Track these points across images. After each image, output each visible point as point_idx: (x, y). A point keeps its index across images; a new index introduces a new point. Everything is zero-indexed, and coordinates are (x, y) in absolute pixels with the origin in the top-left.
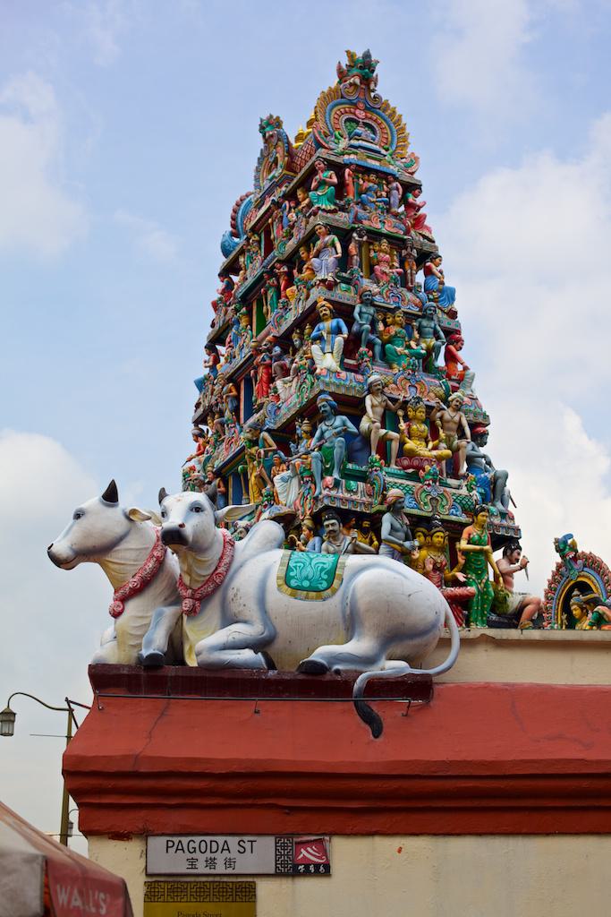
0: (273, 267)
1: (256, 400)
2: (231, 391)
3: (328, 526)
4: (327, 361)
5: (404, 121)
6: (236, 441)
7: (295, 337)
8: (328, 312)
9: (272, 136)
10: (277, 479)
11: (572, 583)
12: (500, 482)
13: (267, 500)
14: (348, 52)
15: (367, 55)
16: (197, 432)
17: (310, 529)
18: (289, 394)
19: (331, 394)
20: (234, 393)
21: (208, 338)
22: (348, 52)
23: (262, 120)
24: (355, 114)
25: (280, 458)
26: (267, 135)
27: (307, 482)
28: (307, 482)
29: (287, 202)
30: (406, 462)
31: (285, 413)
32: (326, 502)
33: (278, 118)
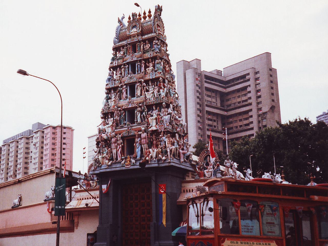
3: (169, 135)
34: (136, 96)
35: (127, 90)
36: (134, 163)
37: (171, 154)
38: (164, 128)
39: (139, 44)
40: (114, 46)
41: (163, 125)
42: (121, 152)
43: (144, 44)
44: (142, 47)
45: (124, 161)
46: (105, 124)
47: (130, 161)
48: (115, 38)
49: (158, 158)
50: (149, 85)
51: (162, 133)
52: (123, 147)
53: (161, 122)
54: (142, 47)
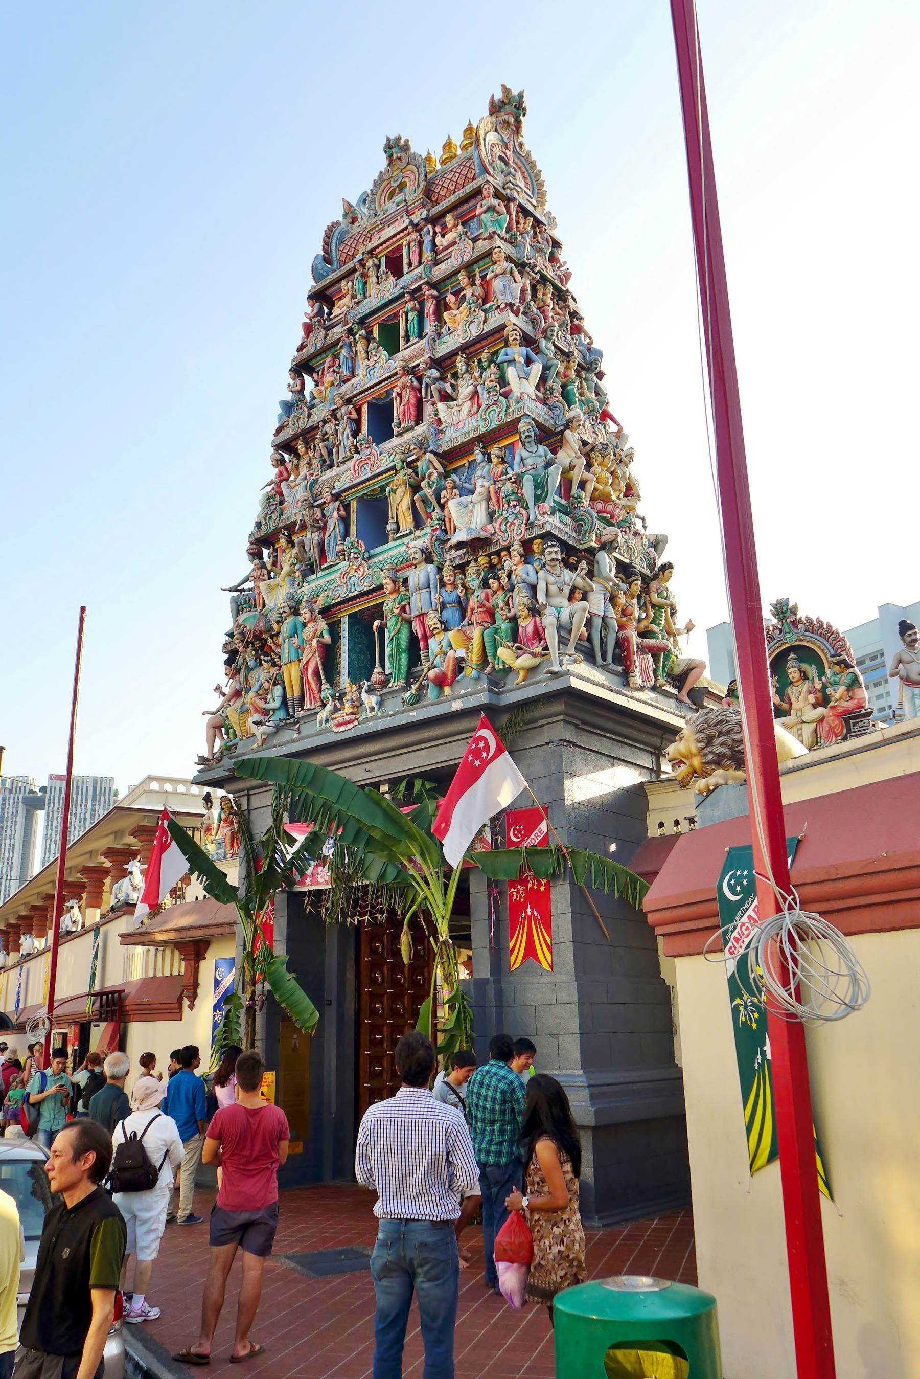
0: (419, 288)
1: (399, 425)
2: (350, 413)
3: (550, 553)
4: (523, 385)
5: (543, 177)
6: (372, 464)
7: (460, 362)
8: (518, 338)
9: (399, 158)
10: (452, 505)
11: (785, 646)
12: (661, 545)
13: (439, 524)
14: (503, 86)
15: (521, 96)
16: (279, 457)
17: (521, 556)
18: (459, 421)
19: (533, 419)
20: (354, 415)
21: (293, 361)
22: (503, 86)
23: (388, 139)
24: (505, 154)
25: (454, 482)
26: (395, 156)
27: (515, 506)
28: (515, 506)
29: (430, 227)
30: (599, 506)
31: (451, 438)
32: (549, 528)
33: (407, 141)
34: (395, 433)
35: (358, 422)
36: (372, 709)
37: (563, 641)
38: (523, 526)
39: (414, 235)
40: (313, 287)
41: (519, 512)
42: (316, 673)
43: (438, 229)
44: (427, 245)
45: (329, 707)
46: (265, 572)
47: (358, 705)
48: (320, 260)
49: (494, 667)
50: (455, 376)
51: (517, 549)
52: (329, 654)
53: (508, 502)
54: (427, 245)
